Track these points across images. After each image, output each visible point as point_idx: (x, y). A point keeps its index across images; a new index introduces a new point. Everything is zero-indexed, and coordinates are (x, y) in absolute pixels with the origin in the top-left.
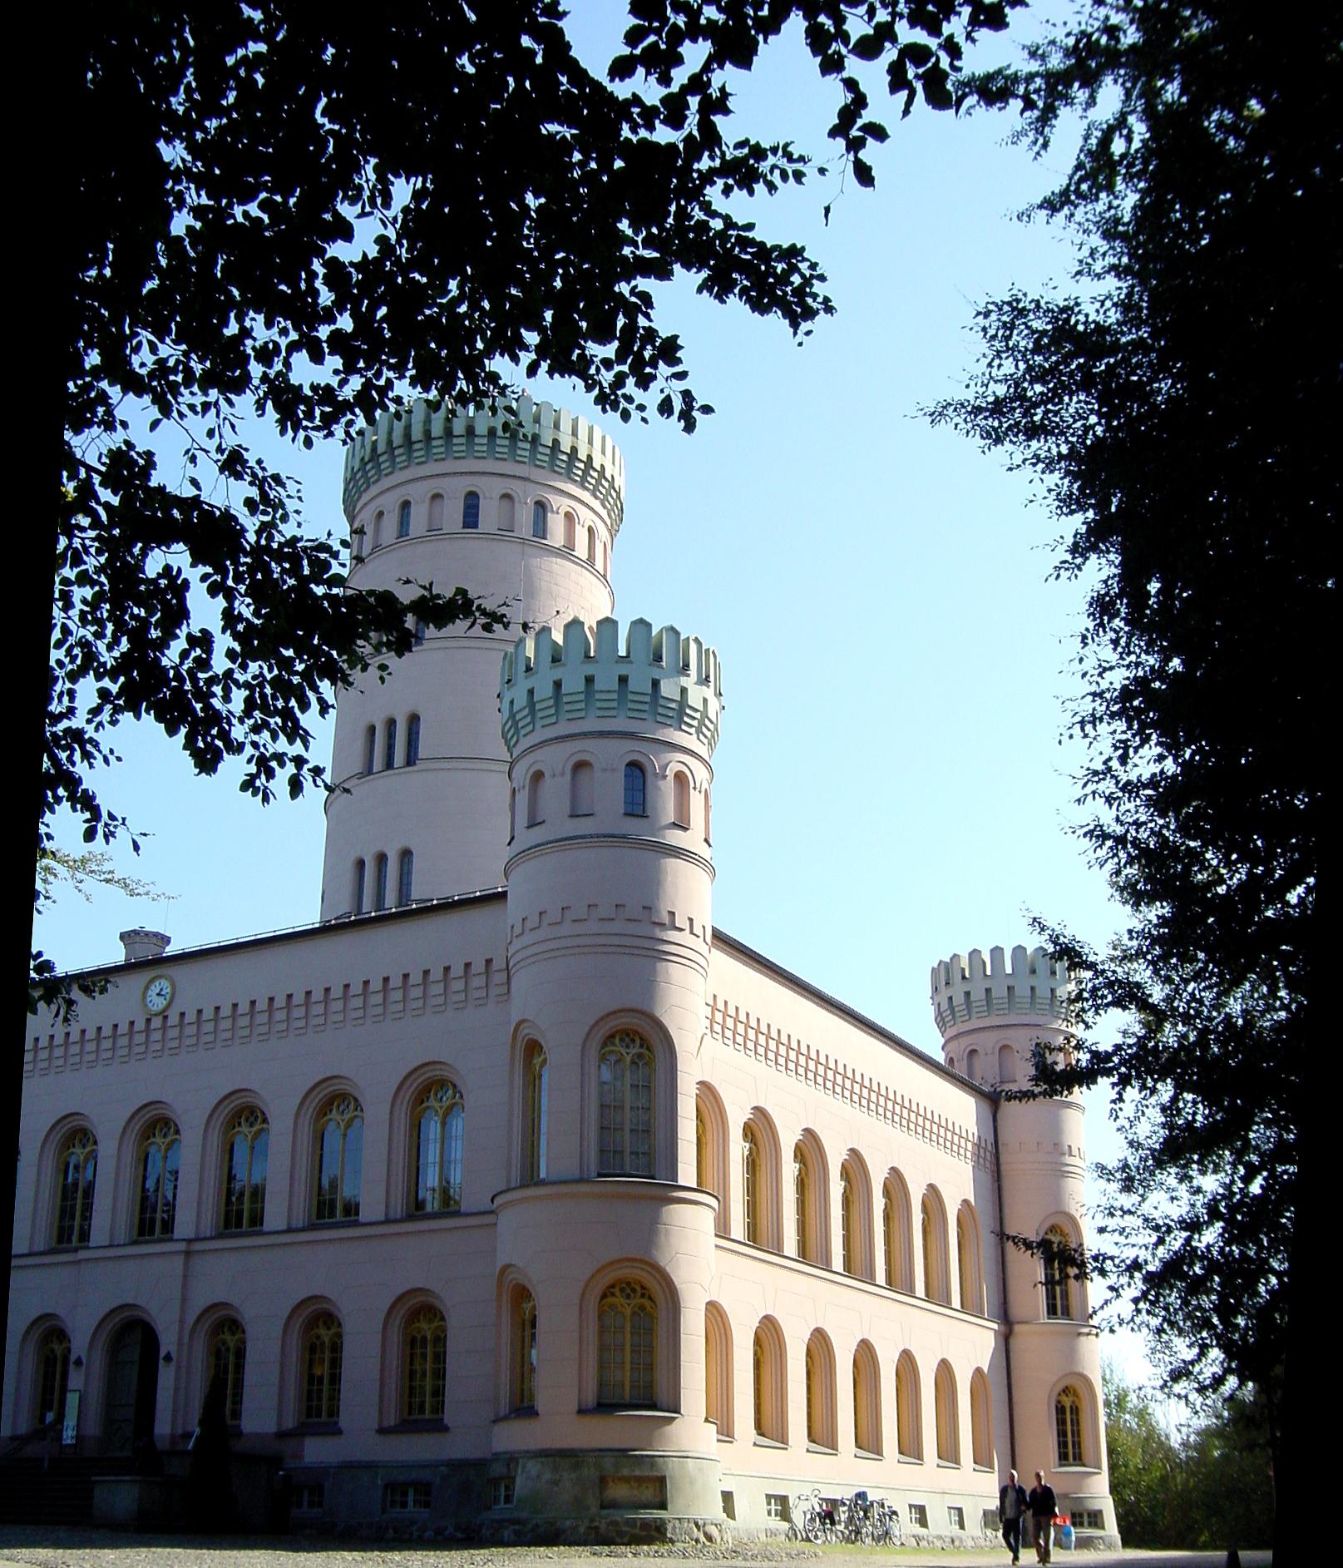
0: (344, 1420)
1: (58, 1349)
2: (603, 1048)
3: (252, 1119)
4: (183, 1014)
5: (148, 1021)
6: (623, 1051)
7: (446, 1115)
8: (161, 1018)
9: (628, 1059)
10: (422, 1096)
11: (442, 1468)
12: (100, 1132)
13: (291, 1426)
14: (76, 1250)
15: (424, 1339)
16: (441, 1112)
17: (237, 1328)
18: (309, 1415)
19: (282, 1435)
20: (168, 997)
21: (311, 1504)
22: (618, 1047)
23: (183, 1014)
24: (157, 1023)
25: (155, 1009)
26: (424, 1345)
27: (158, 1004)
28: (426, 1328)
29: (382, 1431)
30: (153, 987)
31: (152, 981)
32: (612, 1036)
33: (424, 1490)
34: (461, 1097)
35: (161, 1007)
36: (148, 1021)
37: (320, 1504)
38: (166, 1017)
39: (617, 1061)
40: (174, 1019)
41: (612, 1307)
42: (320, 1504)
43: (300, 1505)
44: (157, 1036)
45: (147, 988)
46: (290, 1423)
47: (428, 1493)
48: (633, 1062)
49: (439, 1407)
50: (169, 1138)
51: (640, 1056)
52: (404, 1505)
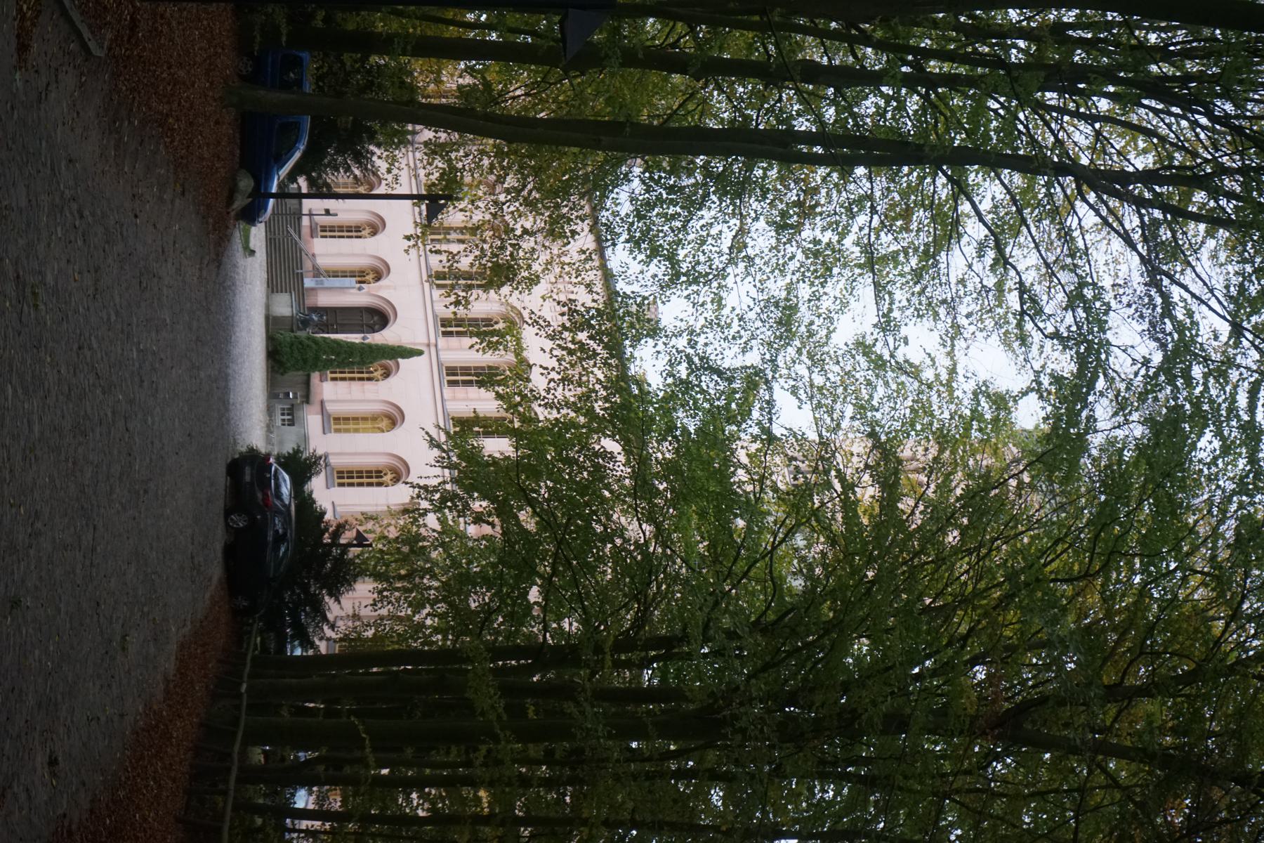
0: (332, 436)
15: (381, 477)
19: (322, 402)
21: (284, 420)
26: (377, 477)
28: (387, 478)
43: (283, 414)
46: (330, 408)
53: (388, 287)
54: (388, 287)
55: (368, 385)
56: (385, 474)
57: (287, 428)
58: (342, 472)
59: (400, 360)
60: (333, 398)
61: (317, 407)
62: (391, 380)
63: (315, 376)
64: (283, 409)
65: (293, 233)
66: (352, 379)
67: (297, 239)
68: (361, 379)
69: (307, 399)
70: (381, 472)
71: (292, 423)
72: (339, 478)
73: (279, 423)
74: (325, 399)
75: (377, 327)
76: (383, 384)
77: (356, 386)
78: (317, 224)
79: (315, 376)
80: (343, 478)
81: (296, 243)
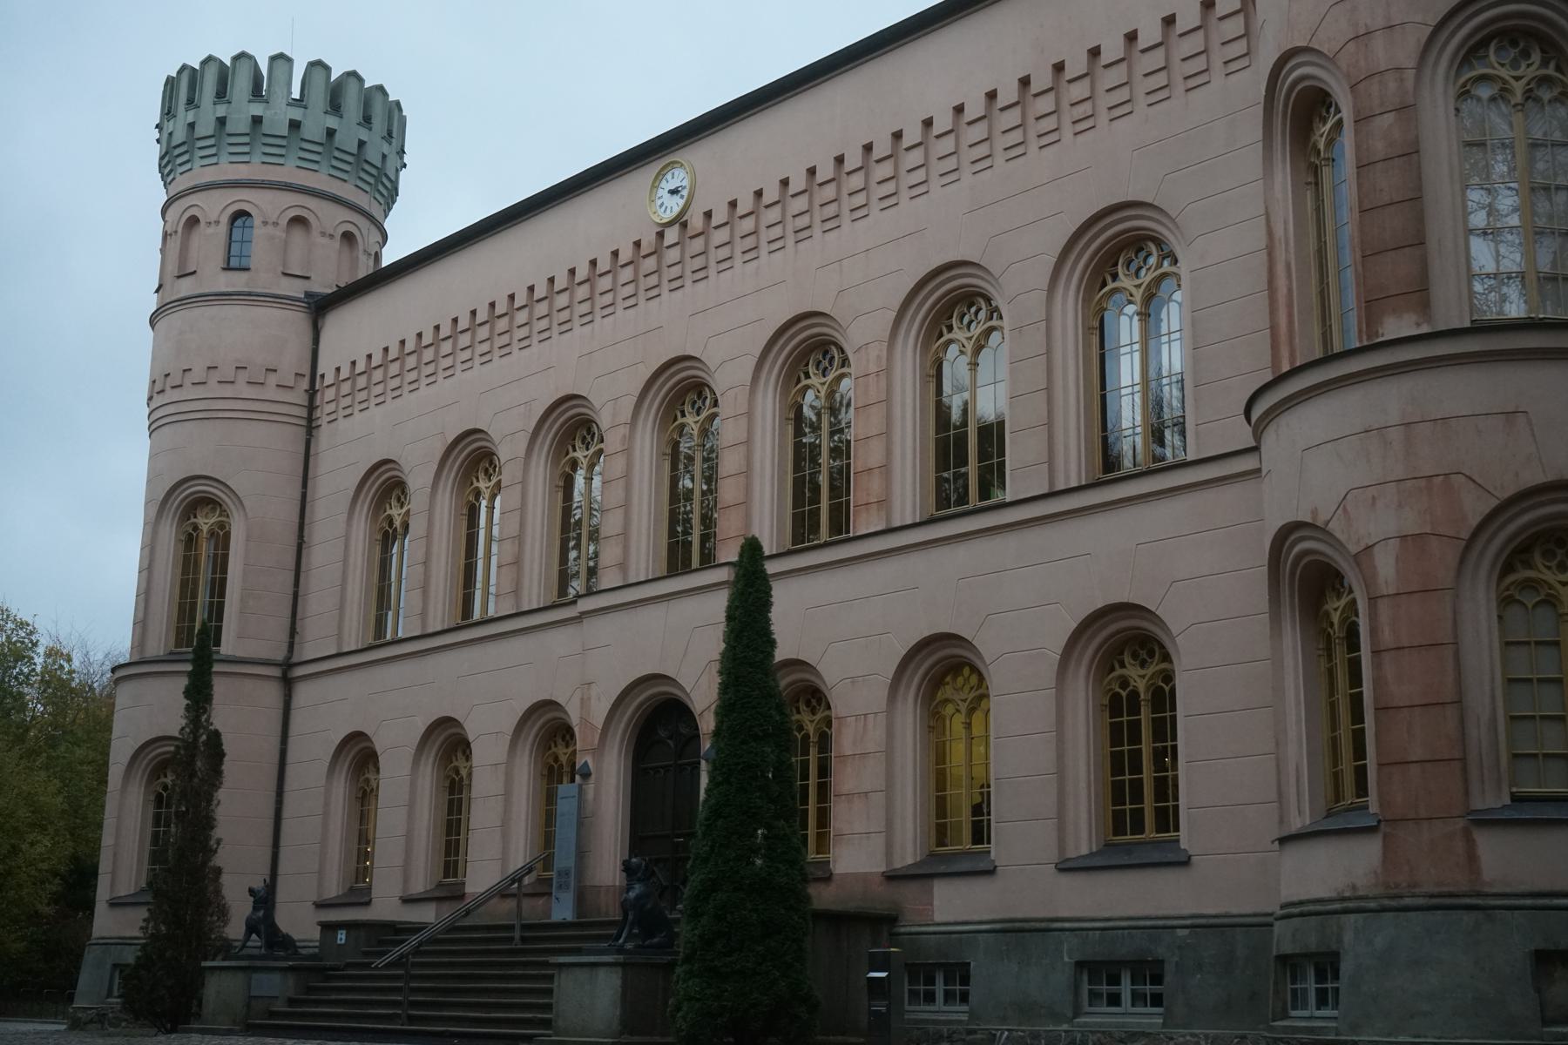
1: (563, 753)
2: (1458, 74)
3: (826, 363)
4: (708, 215)
5: (661, 235)
6: (1504, 73)
7: (1149, 298)
8: (677, 227)
9: (1518, 88)
10: (1102, 272)
11: (1185, 932)
12: (604, 420)
13: (910, 861)
14: (574, 602)
15: (1134, 694)
16: (1138, 295)
17: (819, 701)
18: (941, 843)
19: (892, 877)
20: (685, 193)
21: (949, 996)
22: (1495, 63)
23: (708, 215)
24: (672, 235)
25: (668, 216)
26: (1134, 708)
27: (674, 205)
28: (1139, 677)
29: (1067, 867)
30: (663, 184)
31: (660, 176)
32: (1484, 43)
33: (1149, 971)
34: (1175, 261)
35: (676, 210)
36: (661, 235)
37: (964, 998)
38: (684, 225)
39: (1493, 99)
40: (696, 222)
41: (1530, 585)
42: (964, 998)
43: (930, 998)
44: (673, 255)
45: (655, 186)
46: (907, 856)
47: (1157, 979)
48: (1529, 95)
49: (1167, 819)
50: (704, 414)
51: (1544, 81)
52: (1114, 1000)
53: (584, 702)
54: (584, 702)
55: (845, 741)
56: (1124, 683)
57: (975, 989)
58: (1118, 819)
59: (780, 655)
60: (879, 842)
61: (908, 895)
62: (832, 673)
63: (823, 897)
64: (914, 995)
65: (404, 949)
66: (824, 790)
67: (414, 940)
68: (824, 770)
69: (882, 922)
70: (1115, 698)
71: (959, 973)
72: (1138, 827)
73: (958, 1013)
74: (883, 869)
75: (684, 730)
76: (841, 703)
77: (845, 780)
78: (440, 885)
79: (823, 897)
80: (1138, 816)
81: (433, 941)
